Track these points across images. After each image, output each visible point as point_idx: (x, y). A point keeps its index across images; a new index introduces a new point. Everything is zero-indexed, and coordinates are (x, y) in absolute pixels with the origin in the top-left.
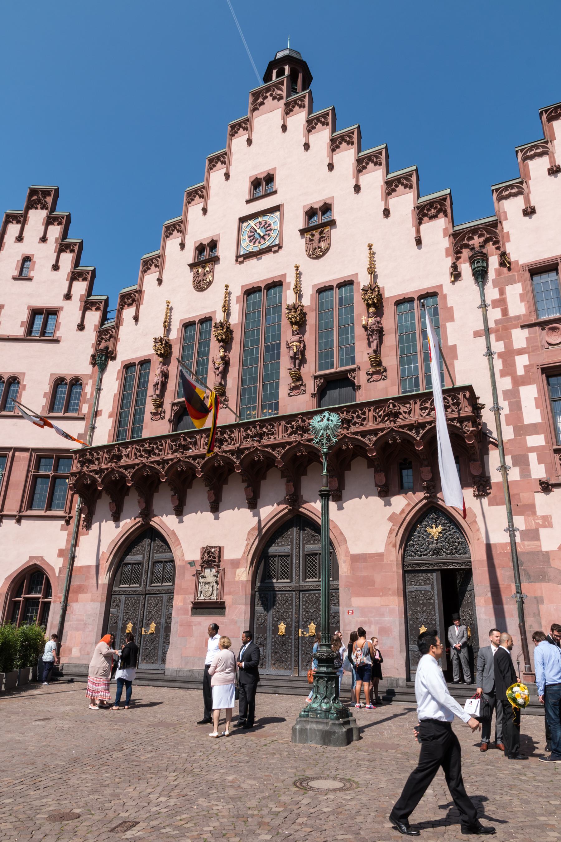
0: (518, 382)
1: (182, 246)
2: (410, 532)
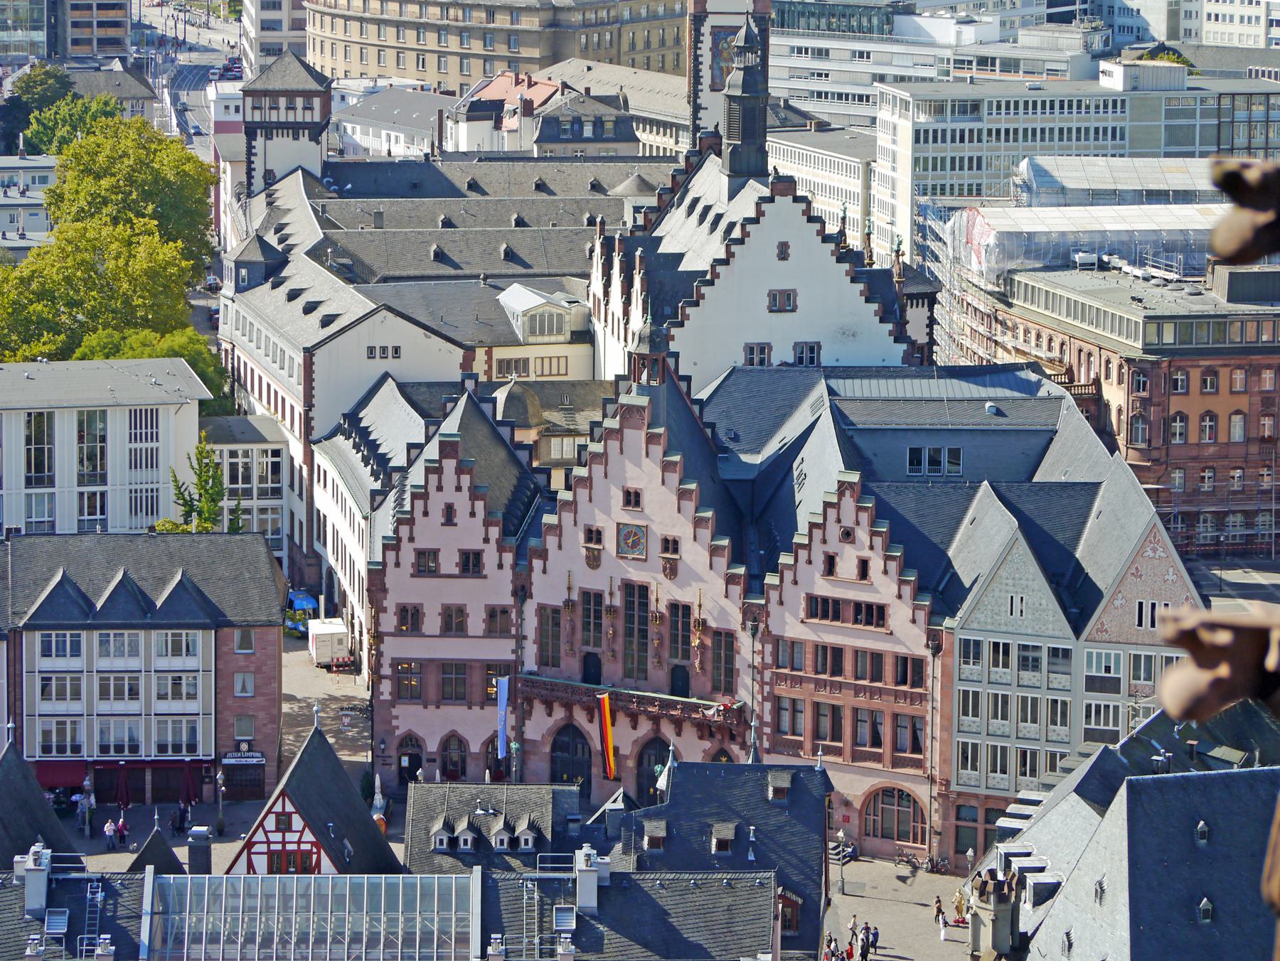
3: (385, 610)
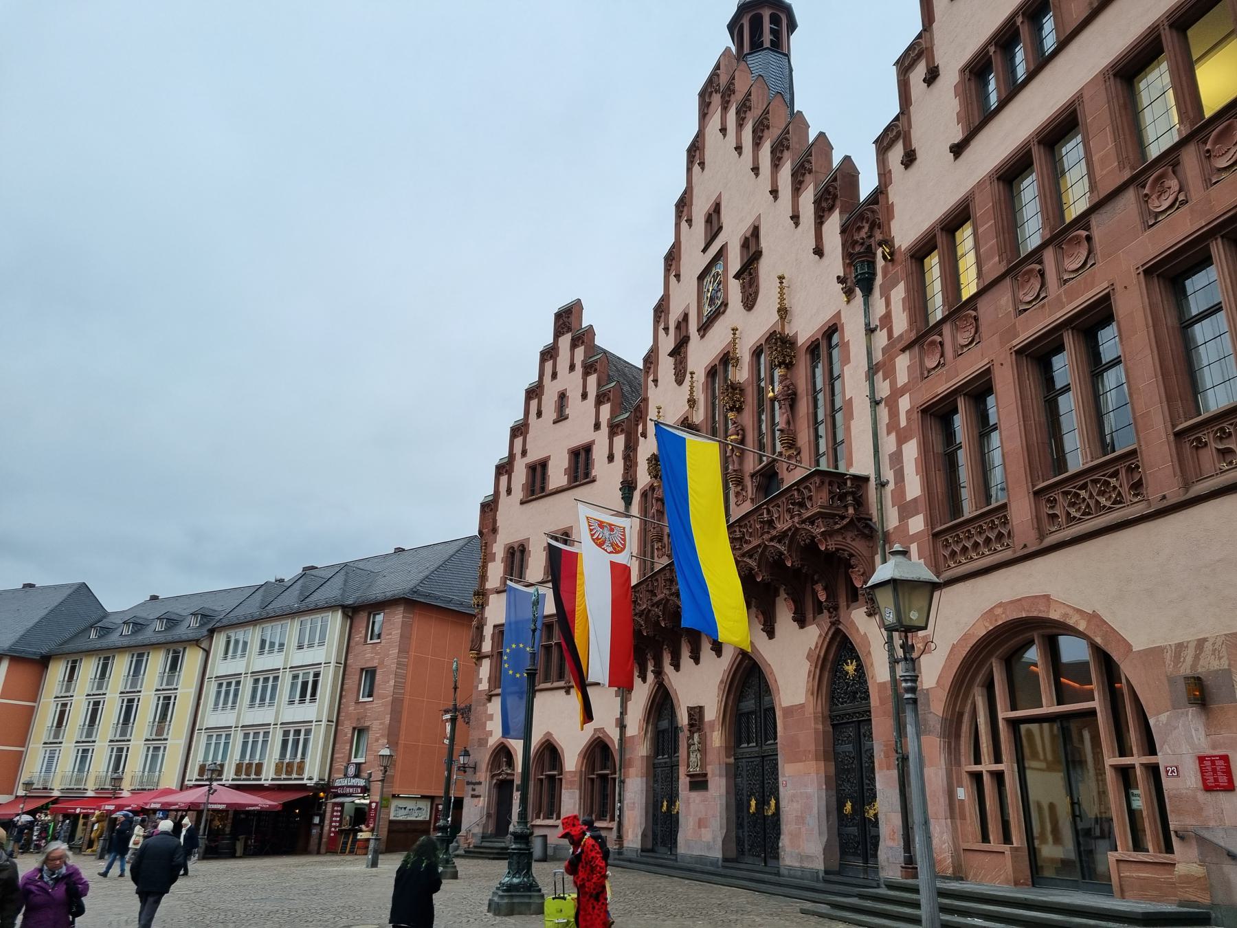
0: (902, 440)
1: (666, 329)
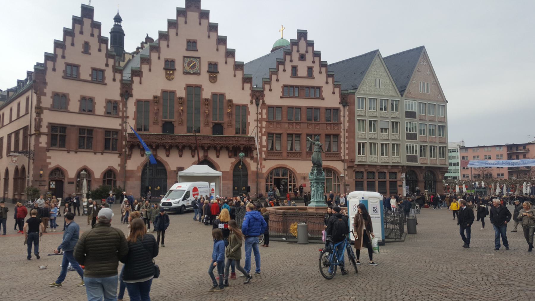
0: (263, 135)
1: (159, 58)
2: (236, 168)
3: (45, 94)
